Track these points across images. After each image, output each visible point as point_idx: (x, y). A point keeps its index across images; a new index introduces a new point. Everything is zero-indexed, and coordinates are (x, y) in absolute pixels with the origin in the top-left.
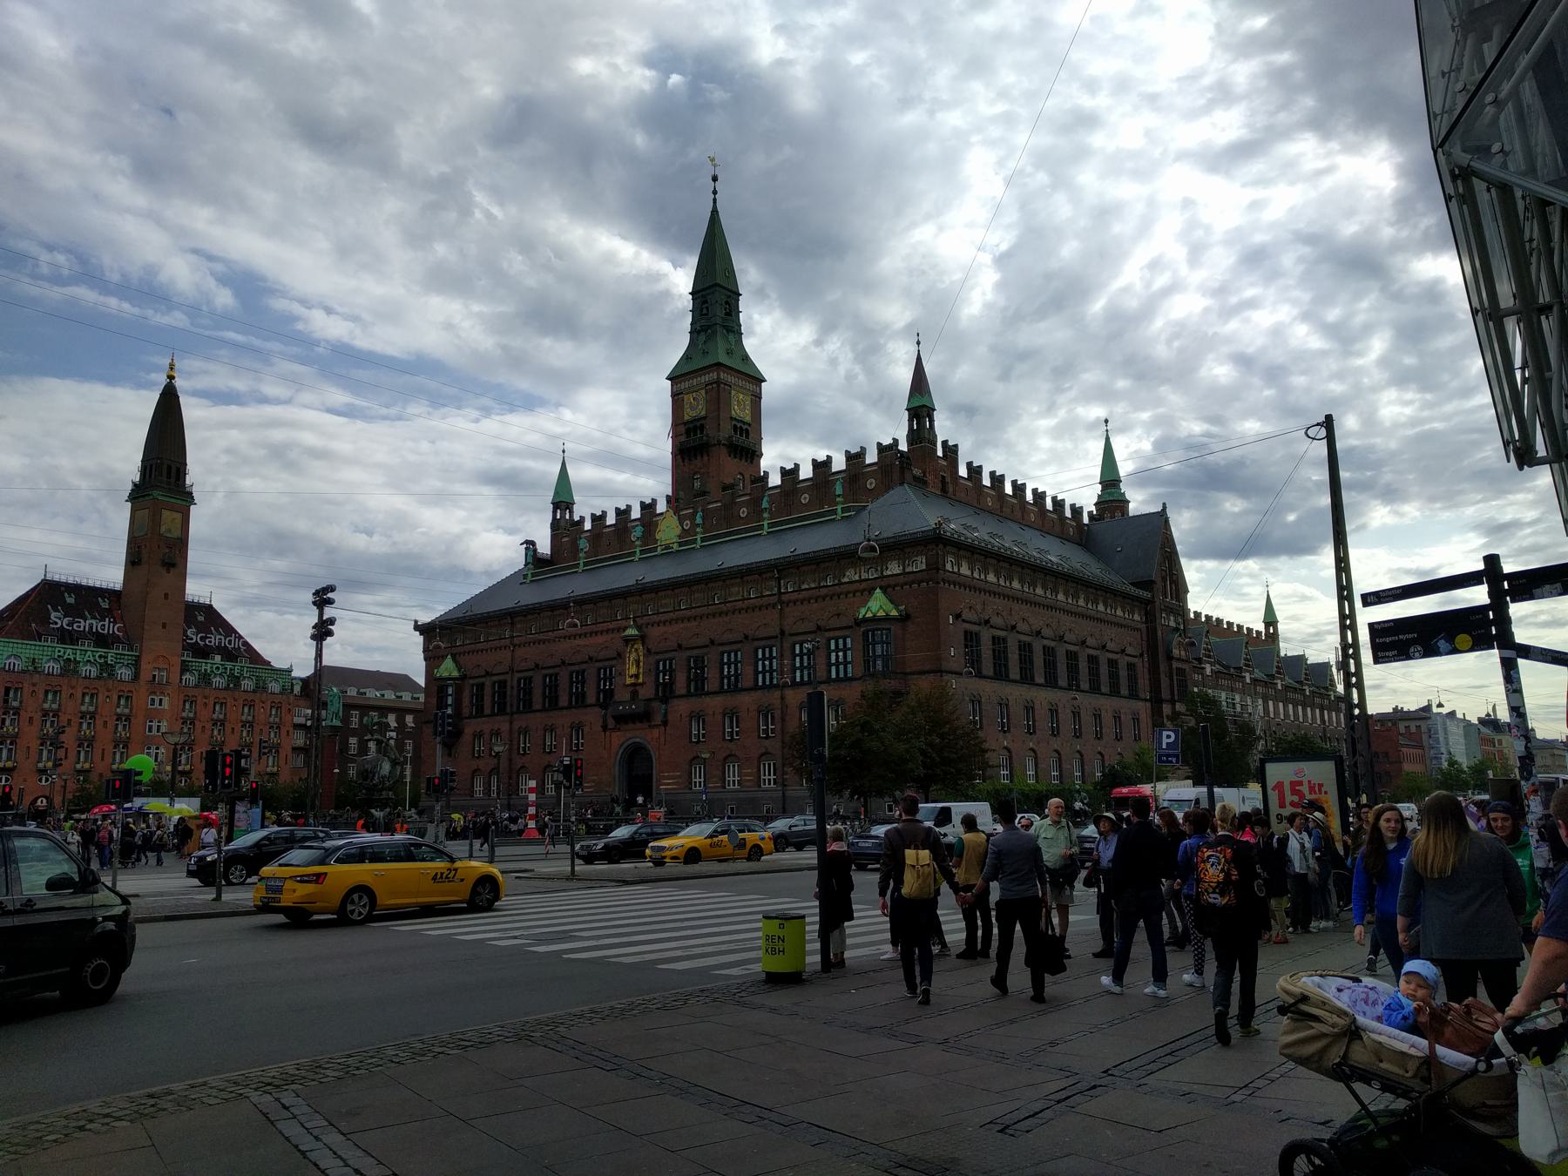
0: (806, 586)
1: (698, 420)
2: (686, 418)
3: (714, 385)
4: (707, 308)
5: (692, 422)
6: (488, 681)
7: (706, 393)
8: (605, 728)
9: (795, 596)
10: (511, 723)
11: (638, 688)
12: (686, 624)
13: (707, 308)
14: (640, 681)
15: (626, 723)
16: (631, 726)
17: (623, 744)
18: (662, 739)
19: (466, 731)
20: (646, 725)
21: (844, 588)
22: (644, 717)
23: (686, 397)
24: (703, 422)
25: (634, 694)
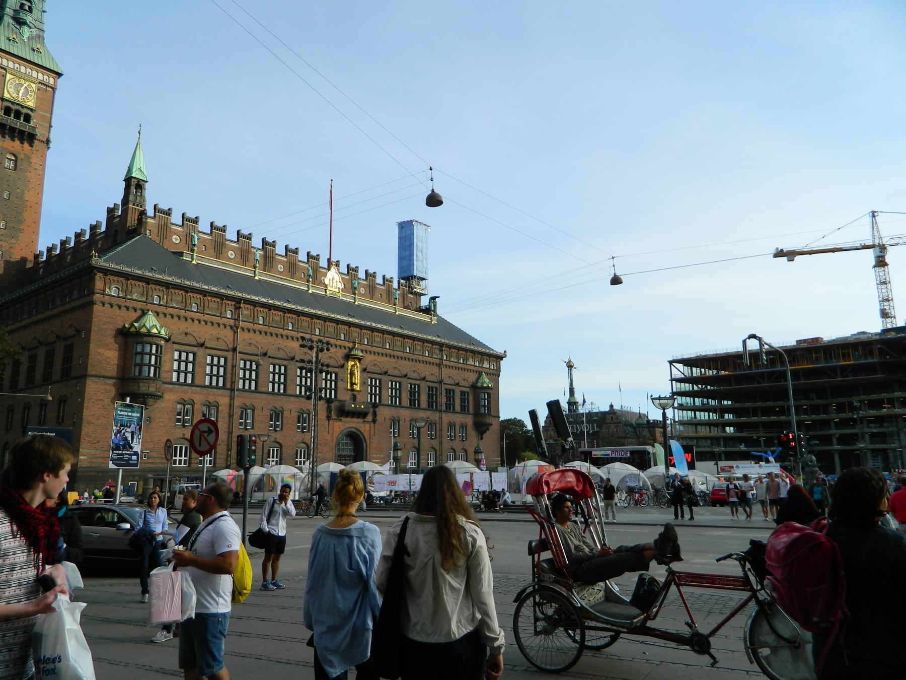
0: (452, 360)
1: (22, 107)
2: (6, 95)
3: (51, 90)
4: (30, 8)
5: (13, 103)
6: (200, 352)
7: (39, 90)
8: (328, 418)
9: (448, 363)
10: (232, 398)
11: (355, 393)
12: (388, 359)
13: (30, 8)
14: (358, 389)
15: (347, 417)
16: (349, 419)
17: (343, 430)
18: (372, 431)
19: (167, 396)
20: (360, 420)
21: (469, 367)
22: (362, 415)
23: (9, 76)
24: (29, 112)
25: (354, 398)
